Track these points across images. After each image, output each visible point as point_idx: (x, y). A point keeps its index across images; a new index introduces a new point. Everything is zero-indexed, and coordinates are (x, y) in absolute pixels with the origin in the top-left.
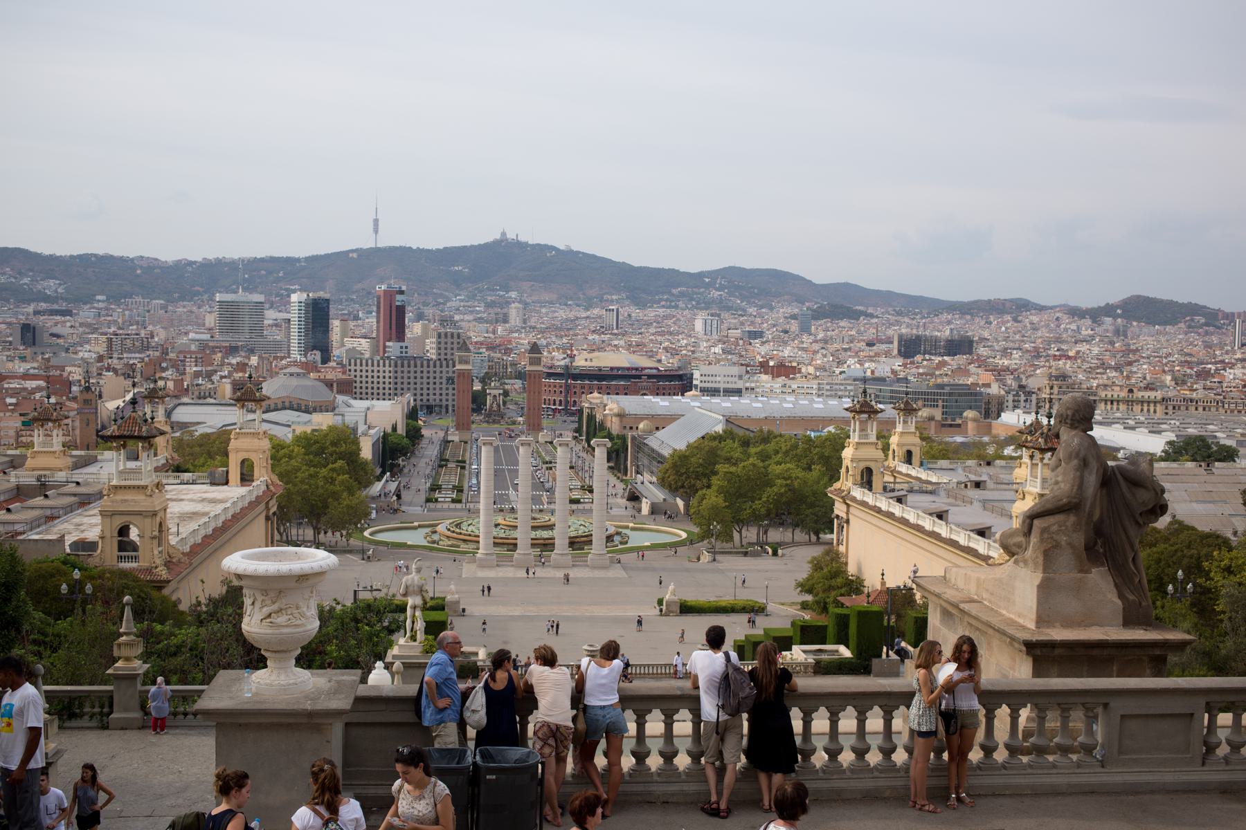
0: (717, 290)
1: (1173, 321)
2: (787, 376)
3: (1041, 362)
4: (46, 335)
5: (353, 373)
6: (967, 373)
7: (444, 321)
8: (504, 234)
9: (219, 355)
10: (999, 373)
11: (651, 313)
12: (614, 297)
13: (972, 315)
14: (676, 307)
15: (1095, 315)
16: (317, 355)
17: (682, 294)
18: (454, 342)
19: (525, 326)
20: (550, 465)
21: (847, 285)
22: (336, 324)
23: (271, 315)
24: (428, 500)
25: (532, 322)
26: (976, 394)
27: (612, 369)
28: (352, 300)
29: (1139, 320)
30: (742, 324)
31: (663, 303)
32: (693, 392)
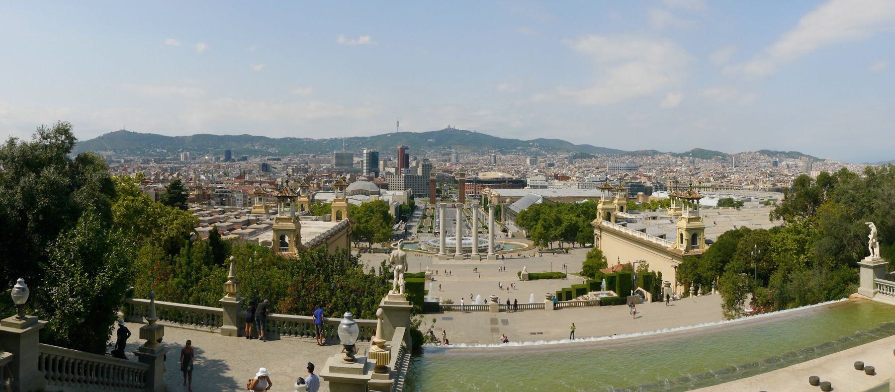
0: (536, 147)
1: (710, 158)
2: (566, 181)
3: (664, 174)
4: (271, 168)
5: (388, 181)
6: (637, 178)
7: (425, 160)
8: (449, 126)
9: (335, 174)
10: (650, 178)
11: (508, 157)
12: (493, 151)
13: (636, 156)
14: (519, 154)
15: (682, 156)
16: (373, 174)
17: (521, 149)
18: (427, 167)
19: (457, 163)
20: (469, 218)
21: (587, 145)
22: (381, 163)
23: (356, 159)
24: (418, 232)
25: (461, 161)
26: (640, 186)
27: (493, 179)
28: (389, 153)
29: (698, 157)
30: (545, 161)
31: (513, 153)
32: (527, 187)
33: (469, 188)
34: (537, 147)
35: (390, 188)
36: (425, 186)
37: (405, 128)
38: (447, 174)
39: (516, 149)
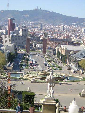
8: (37, 8)
11: (71, 27)
25: (43, 28)
33: (49, 45)
35: (3, 42)
37: (12, 8)
38: (36, 36)
39: (76, 23)
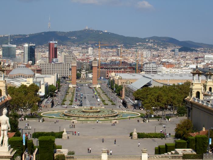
0: (150, 43)
34: (151, 43)
36: (69, 71)
